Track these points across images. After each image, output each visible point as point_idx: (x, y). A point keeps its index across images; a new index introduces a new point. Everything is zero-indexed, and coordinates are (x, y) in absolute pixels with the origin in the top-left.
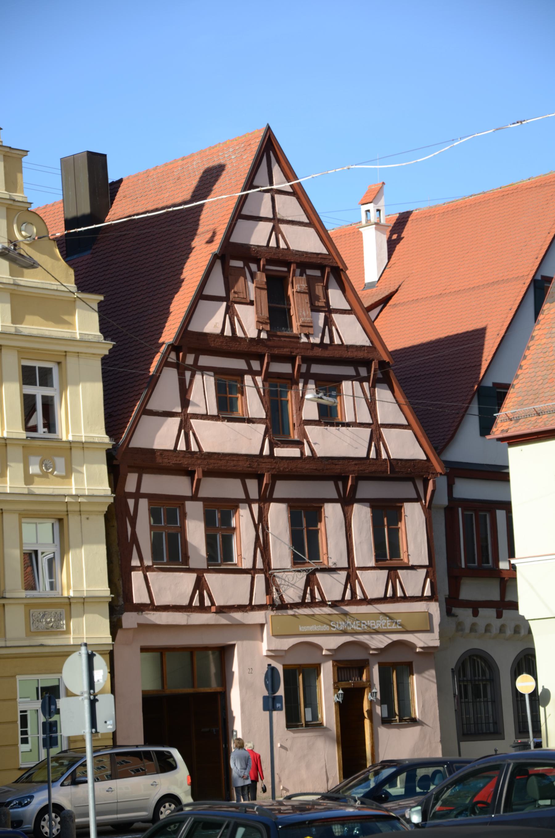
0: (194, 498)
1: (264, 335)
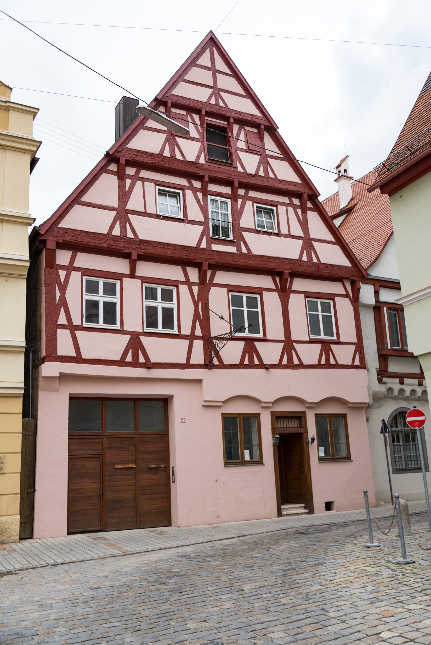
0: (132, 275)
1: (202, 161)
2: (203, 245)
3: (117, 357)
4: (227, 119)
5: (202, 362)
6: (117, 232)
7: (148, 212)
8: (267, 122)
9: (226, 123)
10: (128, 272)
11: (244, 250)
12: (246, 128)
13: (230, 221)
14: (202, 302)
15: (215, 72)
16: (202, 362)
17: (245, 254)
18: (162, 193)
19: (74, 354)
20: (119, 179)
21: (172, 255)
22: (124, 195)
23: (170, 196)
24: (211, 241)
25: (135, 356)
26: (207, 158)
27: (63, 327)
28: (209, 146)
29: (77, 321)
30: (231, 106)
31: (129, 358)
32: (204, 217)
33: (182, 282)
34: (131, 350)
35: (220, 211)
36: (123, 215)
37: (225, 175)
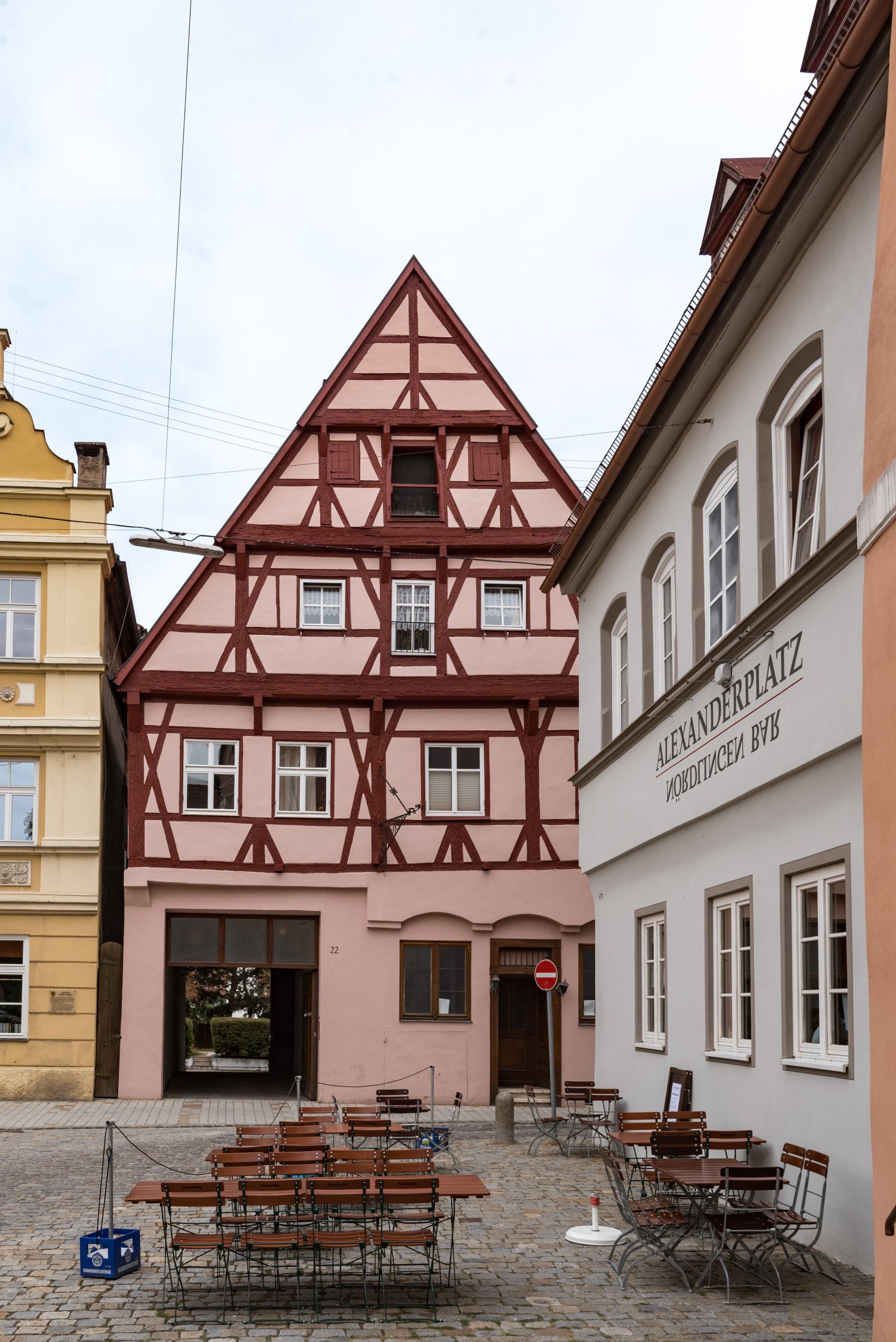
0: (258, 731)
2: (376, 670)
3: (231, 858)
4: (433, 430)
5: (367, 860)
6: (230, 667)
7: (282, 626)
8: (516, 418)
9: (434, 438)
10: (251, 727)
11: (451, 670)
12: (474, 439)
13: (432, 619)
14: (373, 765)
15: (414, 339)
16: (367, 860)
17: (452, 677)
18: (309, 588)
19: (168, 856)
20: (237, 579)
21: (320, 693)
22: (245, 604)
23: (325, 590)
24: (389, 660)
25: (259, 855)
26: (389, 514)
27: (152, 816)
28: (396, 492)
29: (172, 807)
30: (442, 404)
31: (249, 859)
32: (381, 620)
33: (340, 735)
34: (252, 846)
35: (413, 605)
36: (241, 637)
37: (421, 539)
